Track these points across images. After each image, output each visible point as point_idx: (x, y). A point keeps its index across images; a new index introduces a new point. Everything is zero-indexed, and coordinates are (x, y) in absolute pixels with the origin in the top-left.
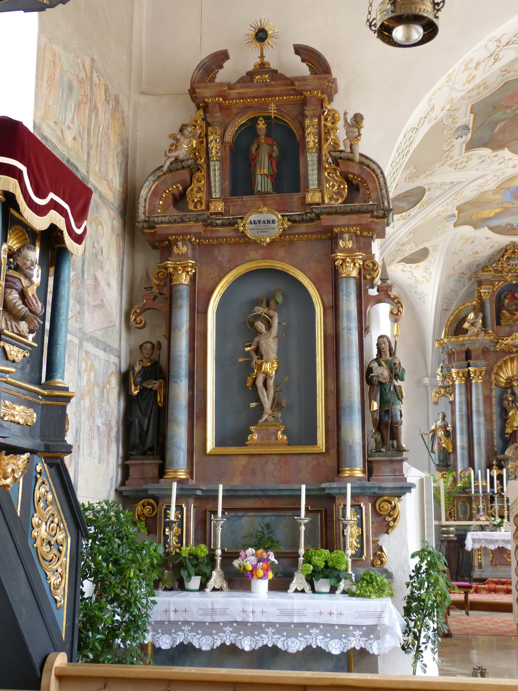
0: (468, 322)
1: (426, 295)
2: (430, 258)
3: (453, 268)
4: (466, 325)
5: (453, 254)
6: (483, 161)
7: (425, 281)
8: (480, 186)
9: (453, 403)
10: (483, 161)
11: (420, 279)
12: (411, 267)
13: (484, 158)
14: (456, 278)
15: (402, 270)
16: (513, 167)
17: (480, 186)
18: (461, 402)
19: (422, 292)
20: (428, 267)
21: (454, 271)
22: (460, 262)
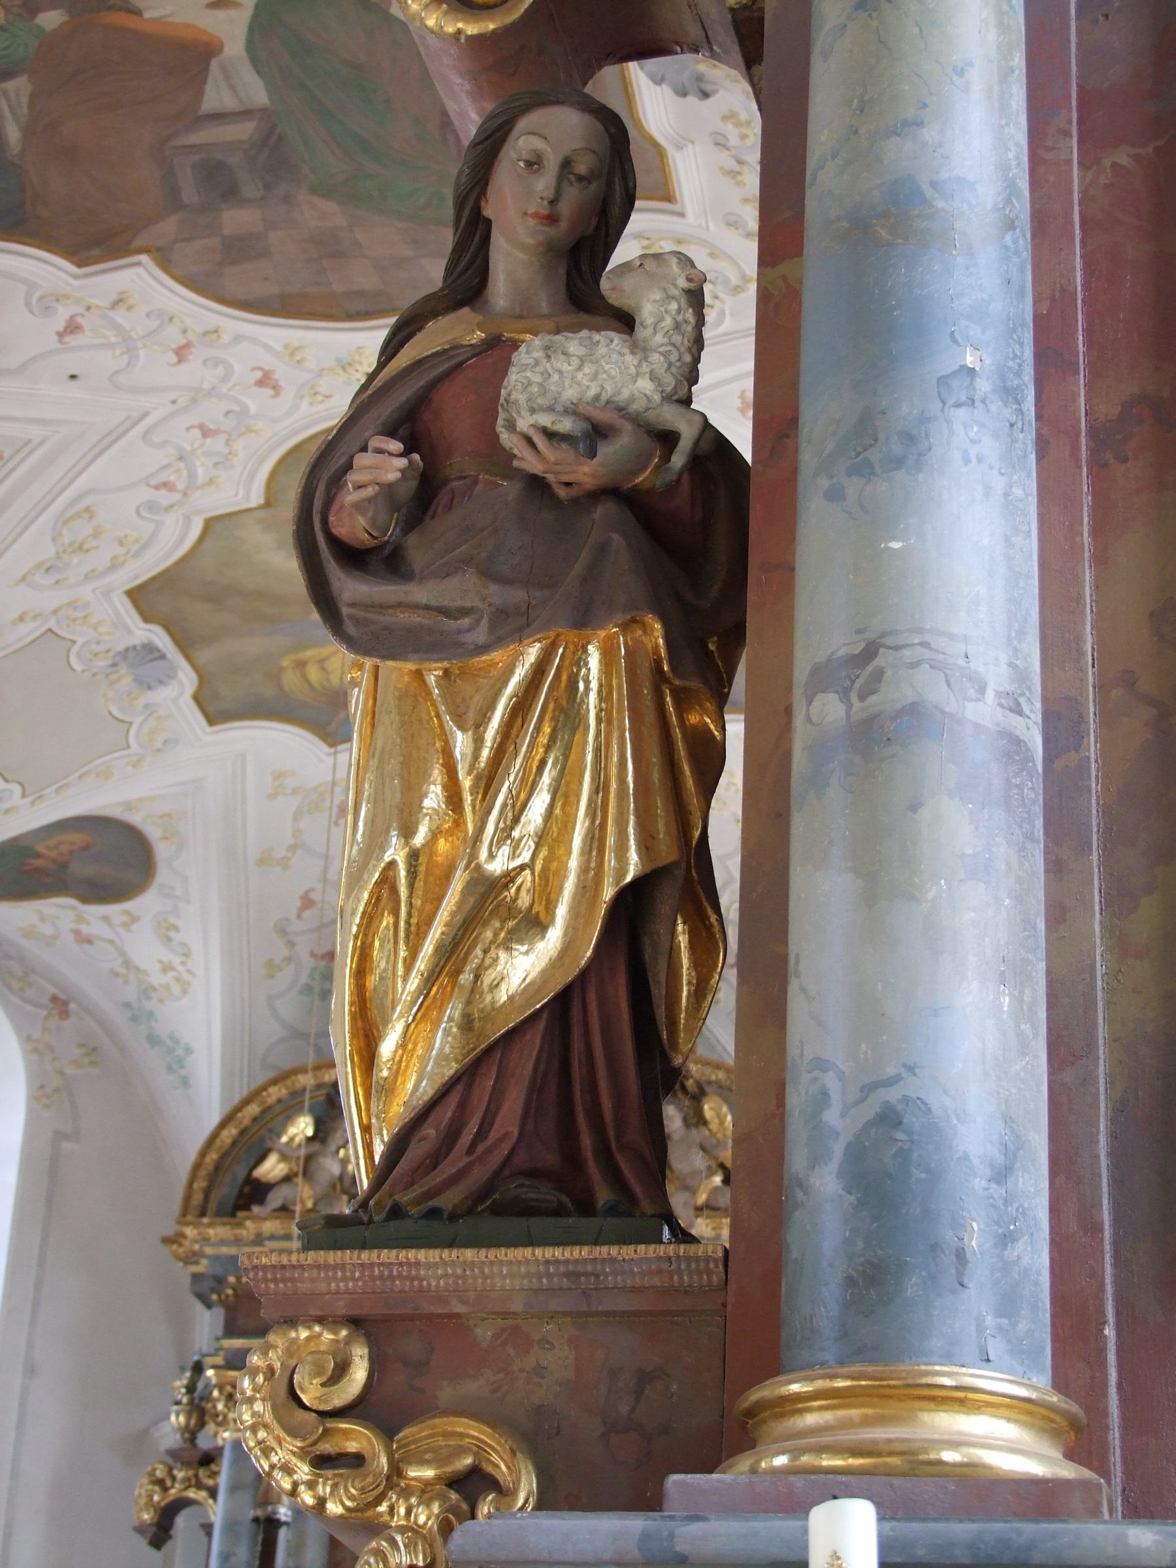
0: (284, 1157)
1: (189, 1050)
2: (163, 874)
3: (282, 930)
4: (271, 1168)
5: (264, 860)
6: (72, 327)
7: (176, 989)
8: (167, 486)
9: (208, 1528)
10: (72, 327)
11: (157, 978)
12: (106, 919)
13: (63, 313)
14: (304, 979)
15: (77, 933)
16: (260, 383)
17: (167, 486)
18: (230, 1526)
19: (172, 1037)
20: (172, 920)
21: (291, 944)
22: (307, 902)
